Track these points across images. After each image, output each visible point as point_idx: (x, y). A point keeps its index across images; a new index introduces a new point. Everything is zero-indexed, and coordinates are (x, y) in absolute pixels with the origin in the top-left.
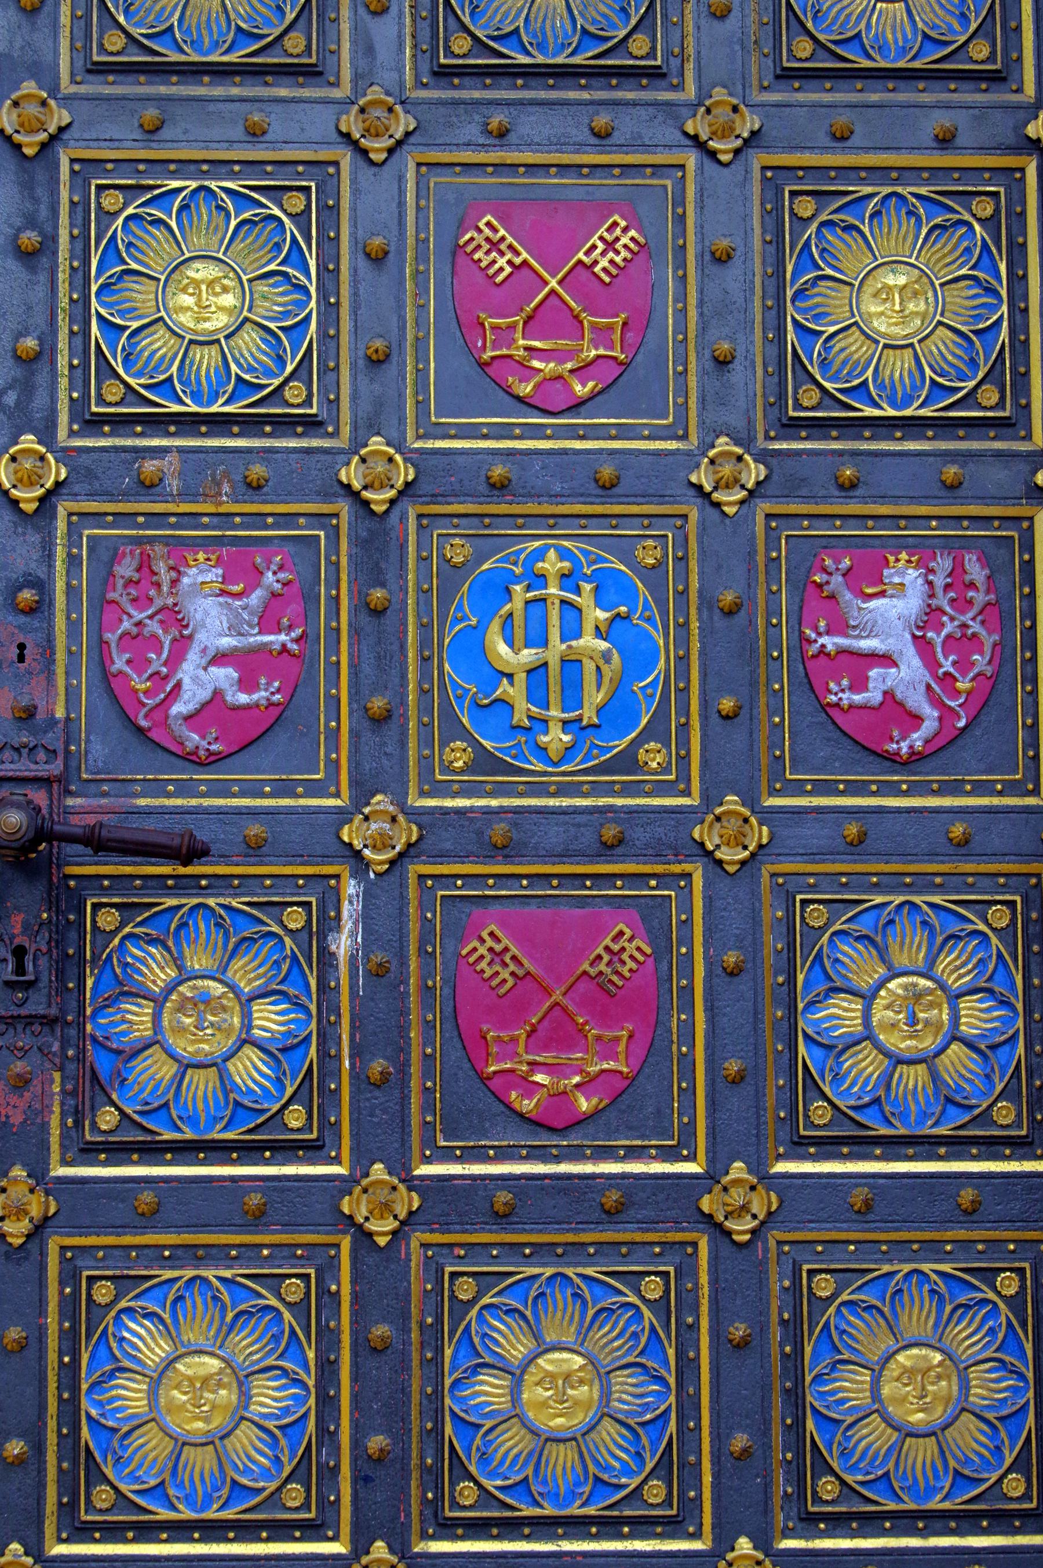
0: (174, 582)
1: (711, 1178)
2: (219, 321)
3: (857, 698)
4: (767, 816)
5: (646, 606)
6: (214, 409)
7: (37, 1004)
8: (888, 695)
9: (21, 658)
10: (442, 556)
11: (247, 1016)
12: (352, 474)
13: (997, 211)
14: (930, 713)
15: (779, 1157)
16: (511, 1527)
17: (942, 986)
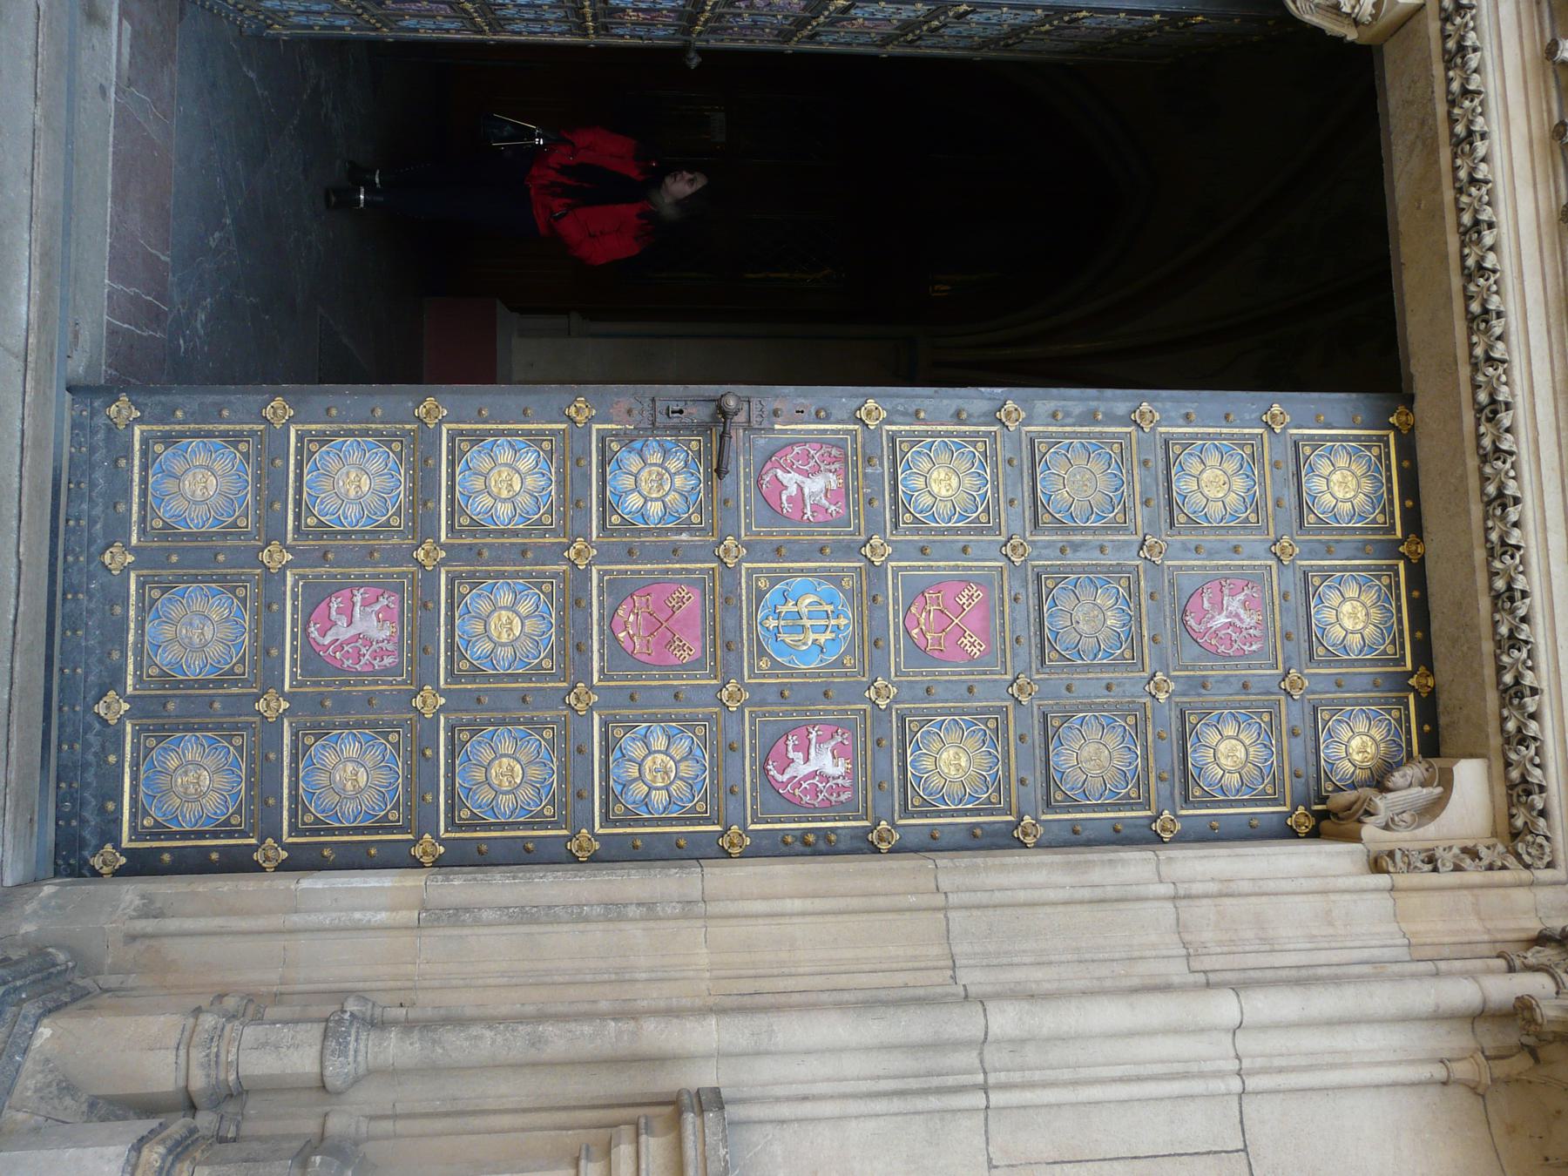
0: (830, 471)
1: (592, 687)
2: (935, 488)
3: (790, 748)
4: (741, 710)
5: (826, 660)
6: (900, 486)
7: (661, 419)
8: (793, 761)
9: (798, 412)
10: (844, 577)
11: (656, 499)
12: (876, 540)
13: (993, 804)
14: (785, 778)
15: (600, 715)
16: (451, 607)
17: (671, 783)
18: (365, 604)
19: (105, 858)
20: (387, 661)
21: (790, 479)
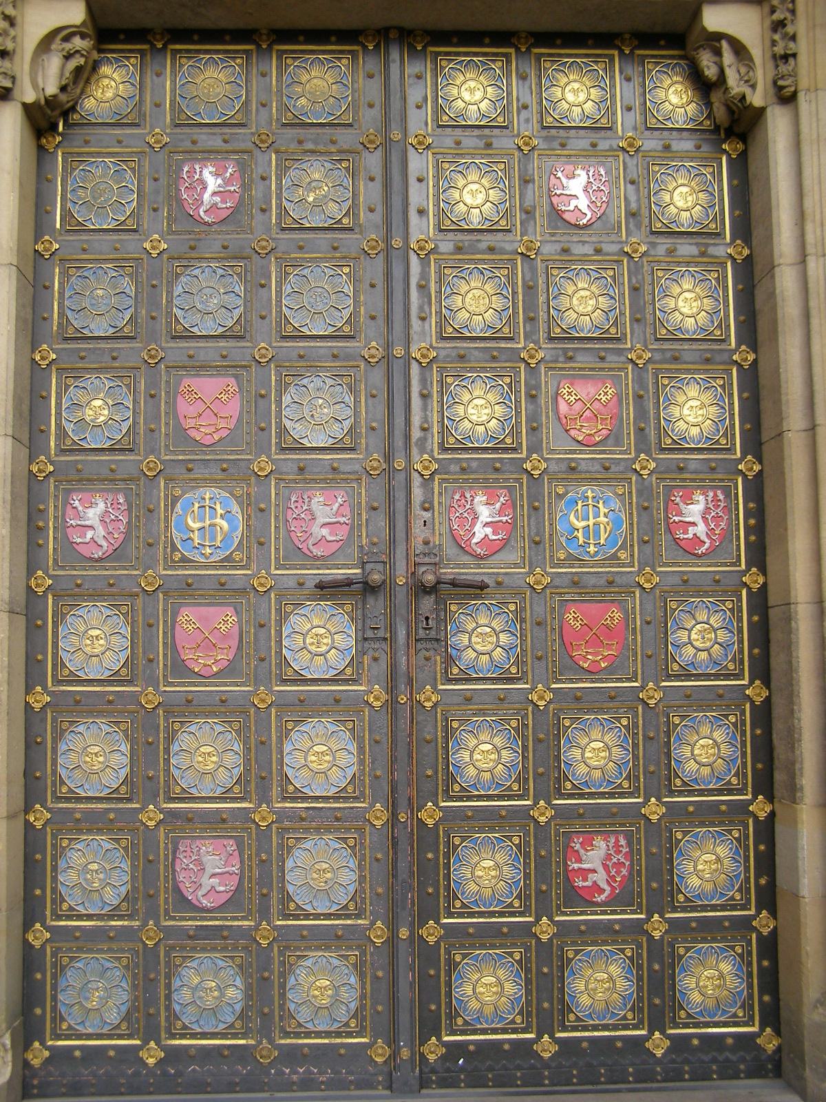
0: (472, 500)
1: (642, 688)
2: (485, 418)
3: (685, 537)
4: (658, 574)
5: (620, 508)
6: (484, 446)
7: (433, 634)
8: (695, 534)
11: (498, 638)
12: (528, 466)
13: (724, 383)
15: (664, 681)
16: (582, 796)
17: (712, 626)
18: (579, 860)
19: (769, 1042)
20: (623, 842)
21: (480, 532)
